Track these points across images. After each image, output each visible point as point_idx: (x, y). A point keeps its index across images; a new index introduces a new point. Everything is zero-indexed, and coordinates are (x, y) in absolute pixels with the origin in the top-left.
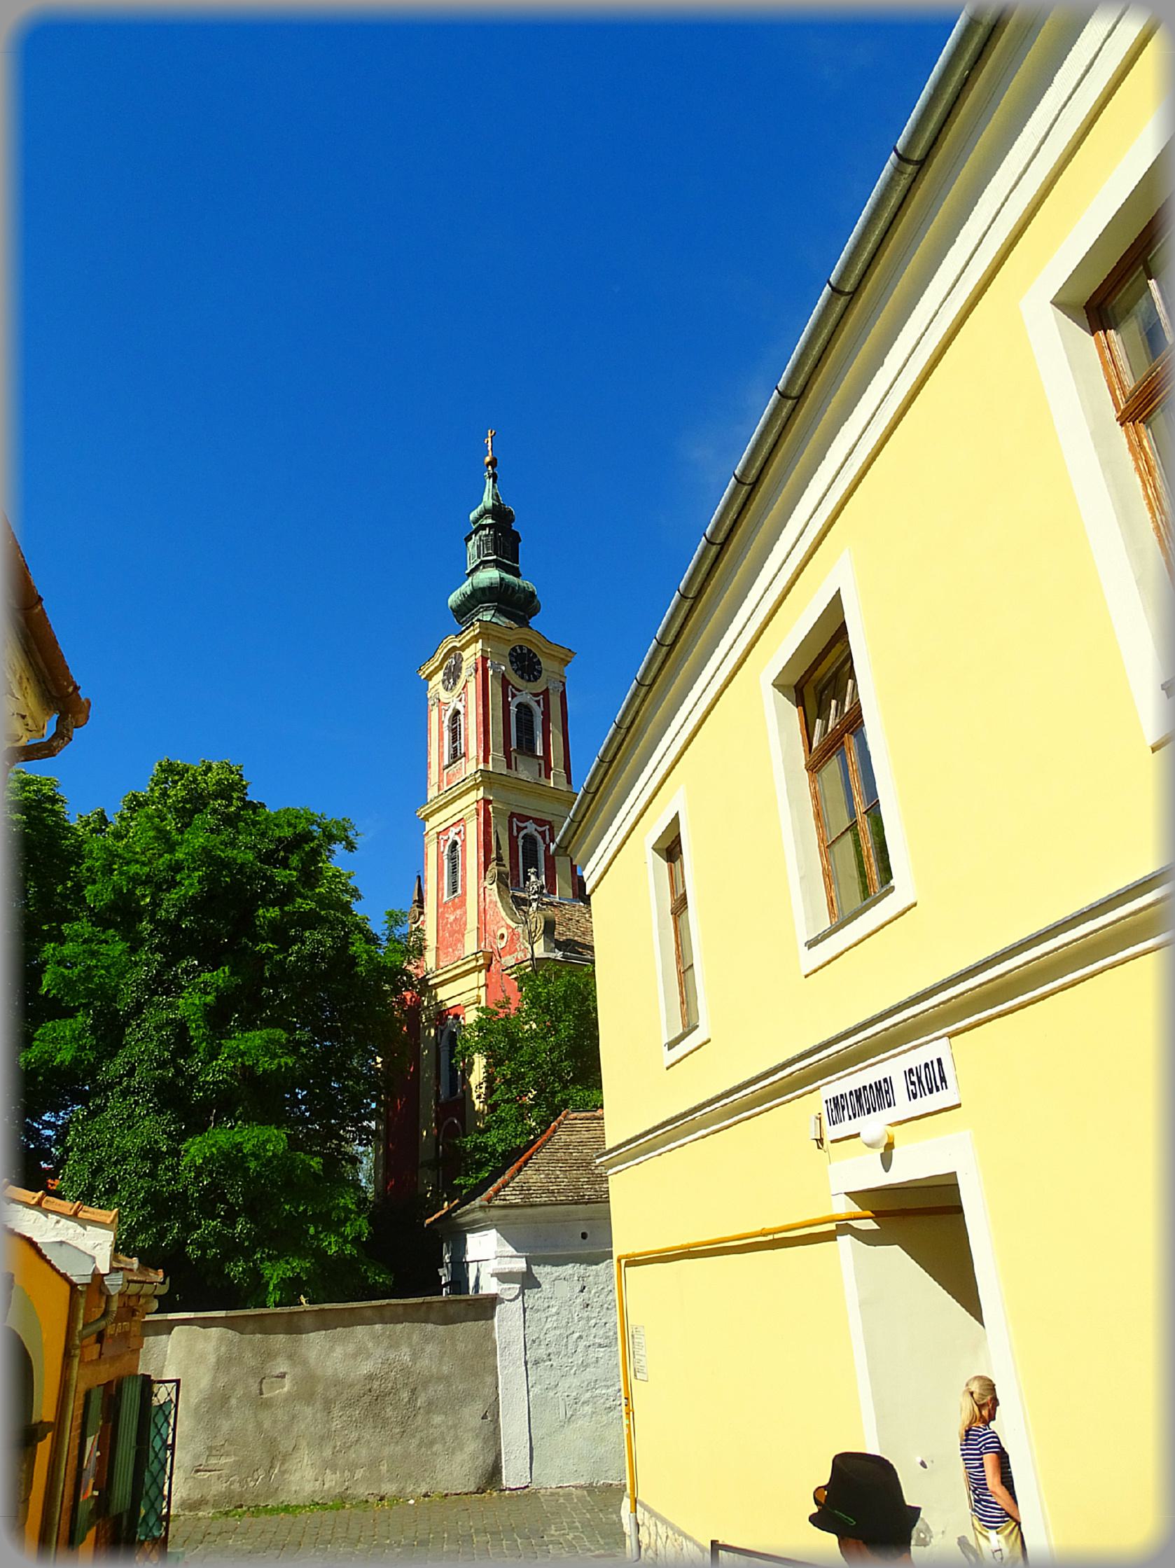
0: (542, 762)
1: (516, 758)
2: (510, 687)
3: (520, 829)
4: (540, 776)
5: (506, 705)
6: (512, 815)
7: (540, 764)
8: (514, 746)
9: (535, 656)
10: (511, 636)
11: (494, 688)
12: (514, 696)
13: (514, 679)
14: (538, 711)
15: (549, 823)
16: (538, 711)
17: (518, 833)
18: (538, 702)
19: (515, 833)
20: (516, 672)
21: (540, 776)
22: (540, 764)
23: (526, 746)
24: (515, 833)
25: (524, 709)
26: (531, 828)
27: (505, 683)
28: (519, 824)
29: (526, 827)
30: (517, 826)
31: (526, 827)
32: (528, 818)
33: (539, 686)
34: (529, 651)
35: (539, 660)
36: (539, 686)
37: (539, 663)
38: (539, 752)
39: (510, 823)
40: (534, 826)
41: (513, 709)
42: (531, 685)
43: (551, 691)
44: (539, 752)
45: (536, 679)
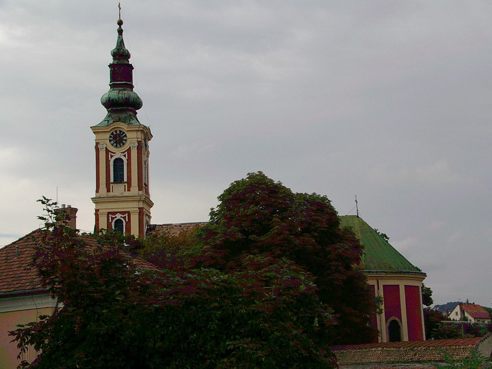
0: (126, 184)
1: (112, 186)
2: (110, 153)
3: (112, 219)
4: (125, 191)
5: (108, 161)
6: (109, 213)
7: (125, 186)
8: (112, 180)
9: (124, 133)
10: (108, 129)
11: (103, 154)
12: (112, 156)
13: (111, 148)
14: (125, 160)
15: (129, 213)
16: (125, 160)
17: (112, 220)
18: (125, 156)
19: (110, 221)
20: (112, 145)
21: (125, 191)
22: (125, 186)
23: (119, 179)
24: (110, 221)
25: (118, 162)
26: (119, 216)
27: (107, 151)
28: (112, 216)
29: (116, 217)
30: (111, 217)
31: (116, 217)
32: (117, 213)
33: (126, 147)
34: (120, 131)
35: (126, 134)
36: (126, 147)
37: (126, 136)
38: (125, 180)
39: (108, 217)
40: (120, 215)
41: (112, 163)
42: (120, 149)
43: (131, 148)
44: (125, 180)
45: (124, 144)
